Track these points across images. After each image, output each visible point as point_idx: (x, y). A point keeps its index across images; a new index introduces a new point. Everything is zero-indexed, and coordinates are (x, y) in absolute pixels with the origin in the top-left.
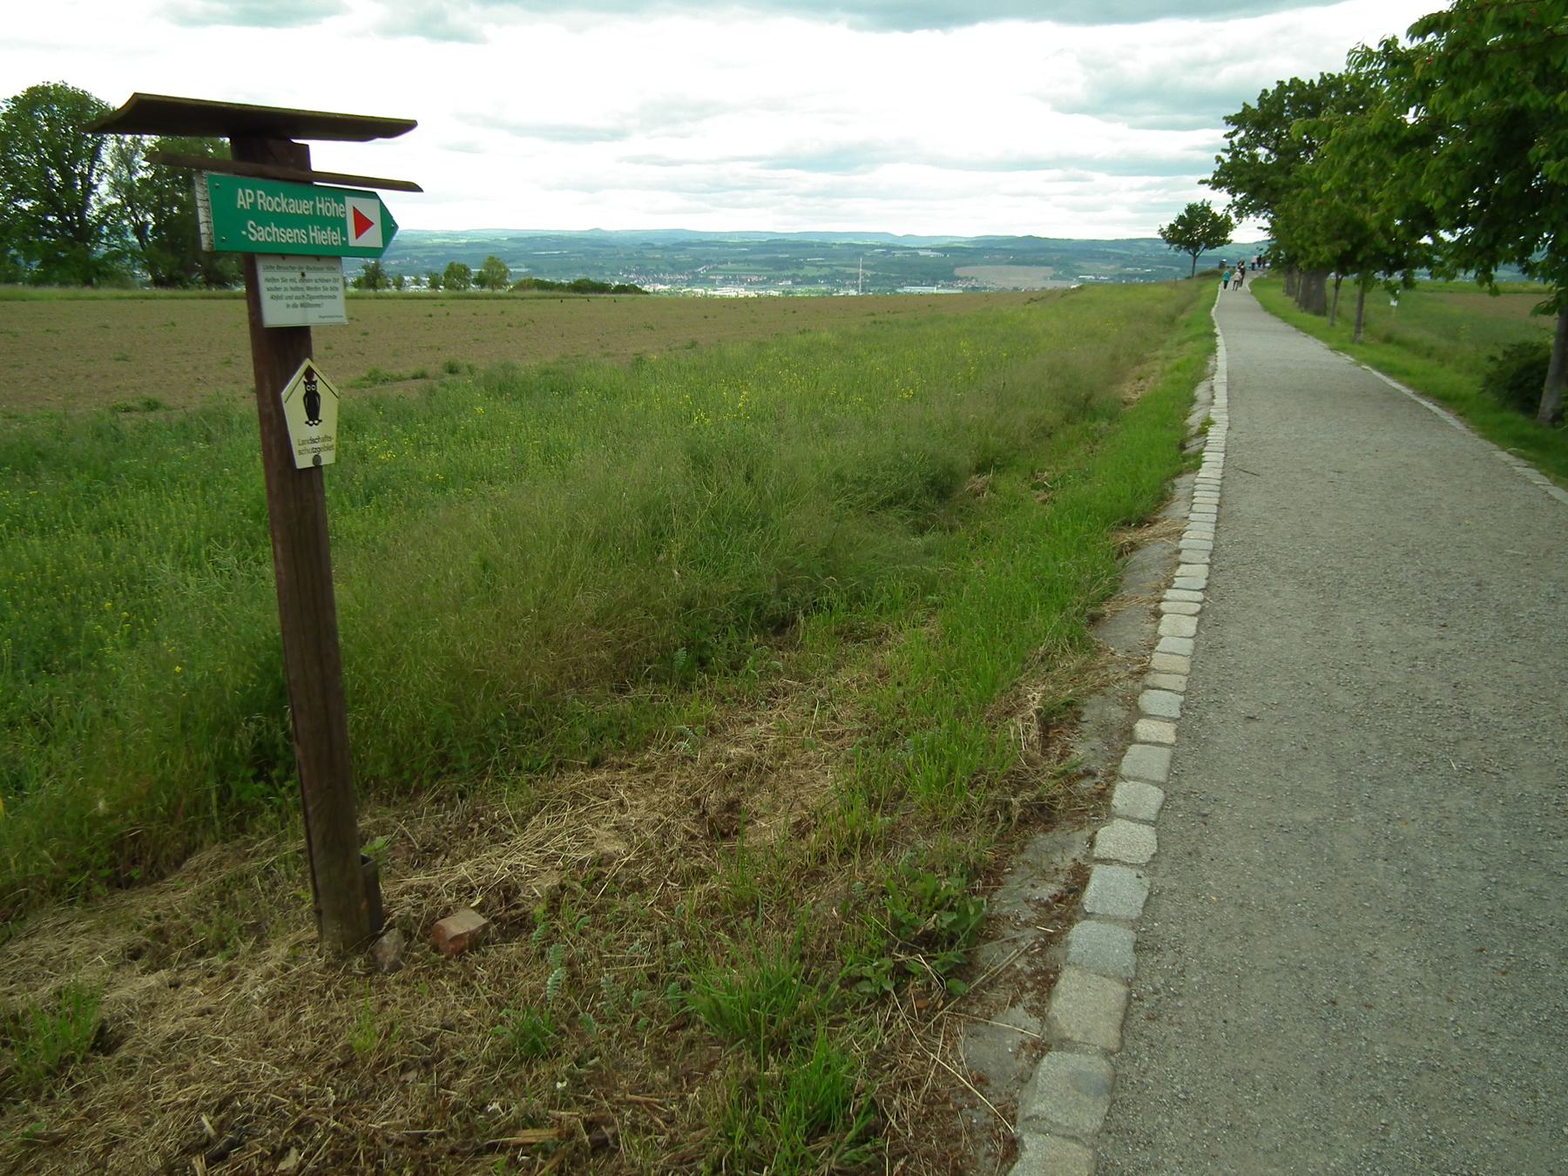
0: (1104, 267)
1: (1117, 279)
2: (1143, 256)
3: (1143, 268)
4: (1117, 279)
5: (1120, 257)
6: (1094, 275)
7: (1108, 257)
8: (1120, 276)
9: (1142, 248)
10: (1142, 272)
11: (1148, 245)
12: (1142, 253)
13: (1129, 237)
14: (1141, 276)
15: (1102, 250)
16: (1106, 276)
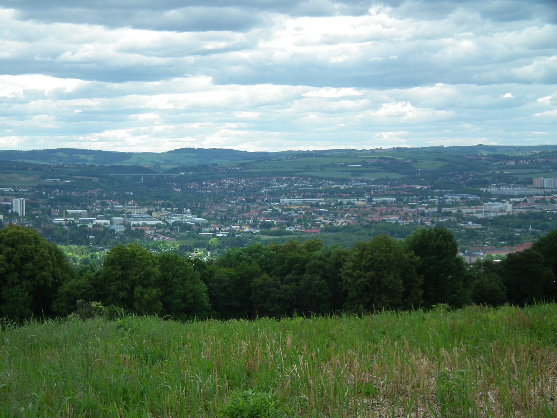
0: (23, 179)
1: (37, 191)
2: (60, 167)
3: (62, 179)
4: (37, 191)
5: (37, 168)
6: (13, 187)
7: (26, 169)
8: (39, 187)
9: (60, 159)
10: (62, 183)
11: (66, 156)
12: (61, 163)
13: (46, 148)
14: (61, 188)
15: (21, 161)
16: (24, 188)
